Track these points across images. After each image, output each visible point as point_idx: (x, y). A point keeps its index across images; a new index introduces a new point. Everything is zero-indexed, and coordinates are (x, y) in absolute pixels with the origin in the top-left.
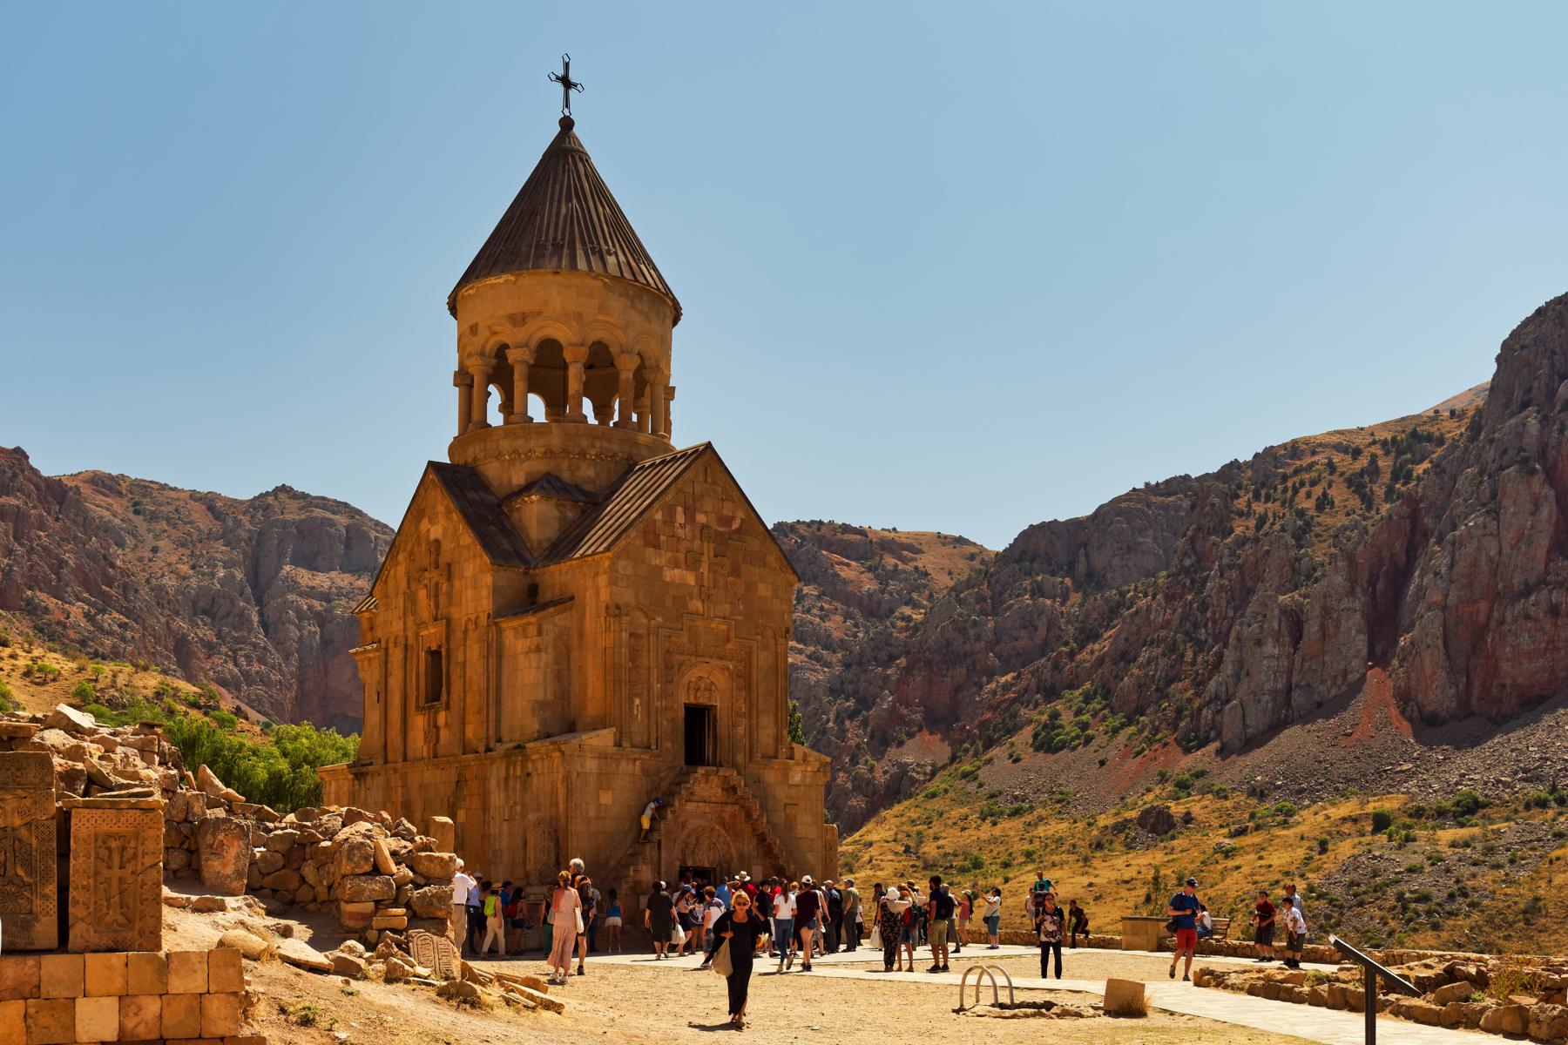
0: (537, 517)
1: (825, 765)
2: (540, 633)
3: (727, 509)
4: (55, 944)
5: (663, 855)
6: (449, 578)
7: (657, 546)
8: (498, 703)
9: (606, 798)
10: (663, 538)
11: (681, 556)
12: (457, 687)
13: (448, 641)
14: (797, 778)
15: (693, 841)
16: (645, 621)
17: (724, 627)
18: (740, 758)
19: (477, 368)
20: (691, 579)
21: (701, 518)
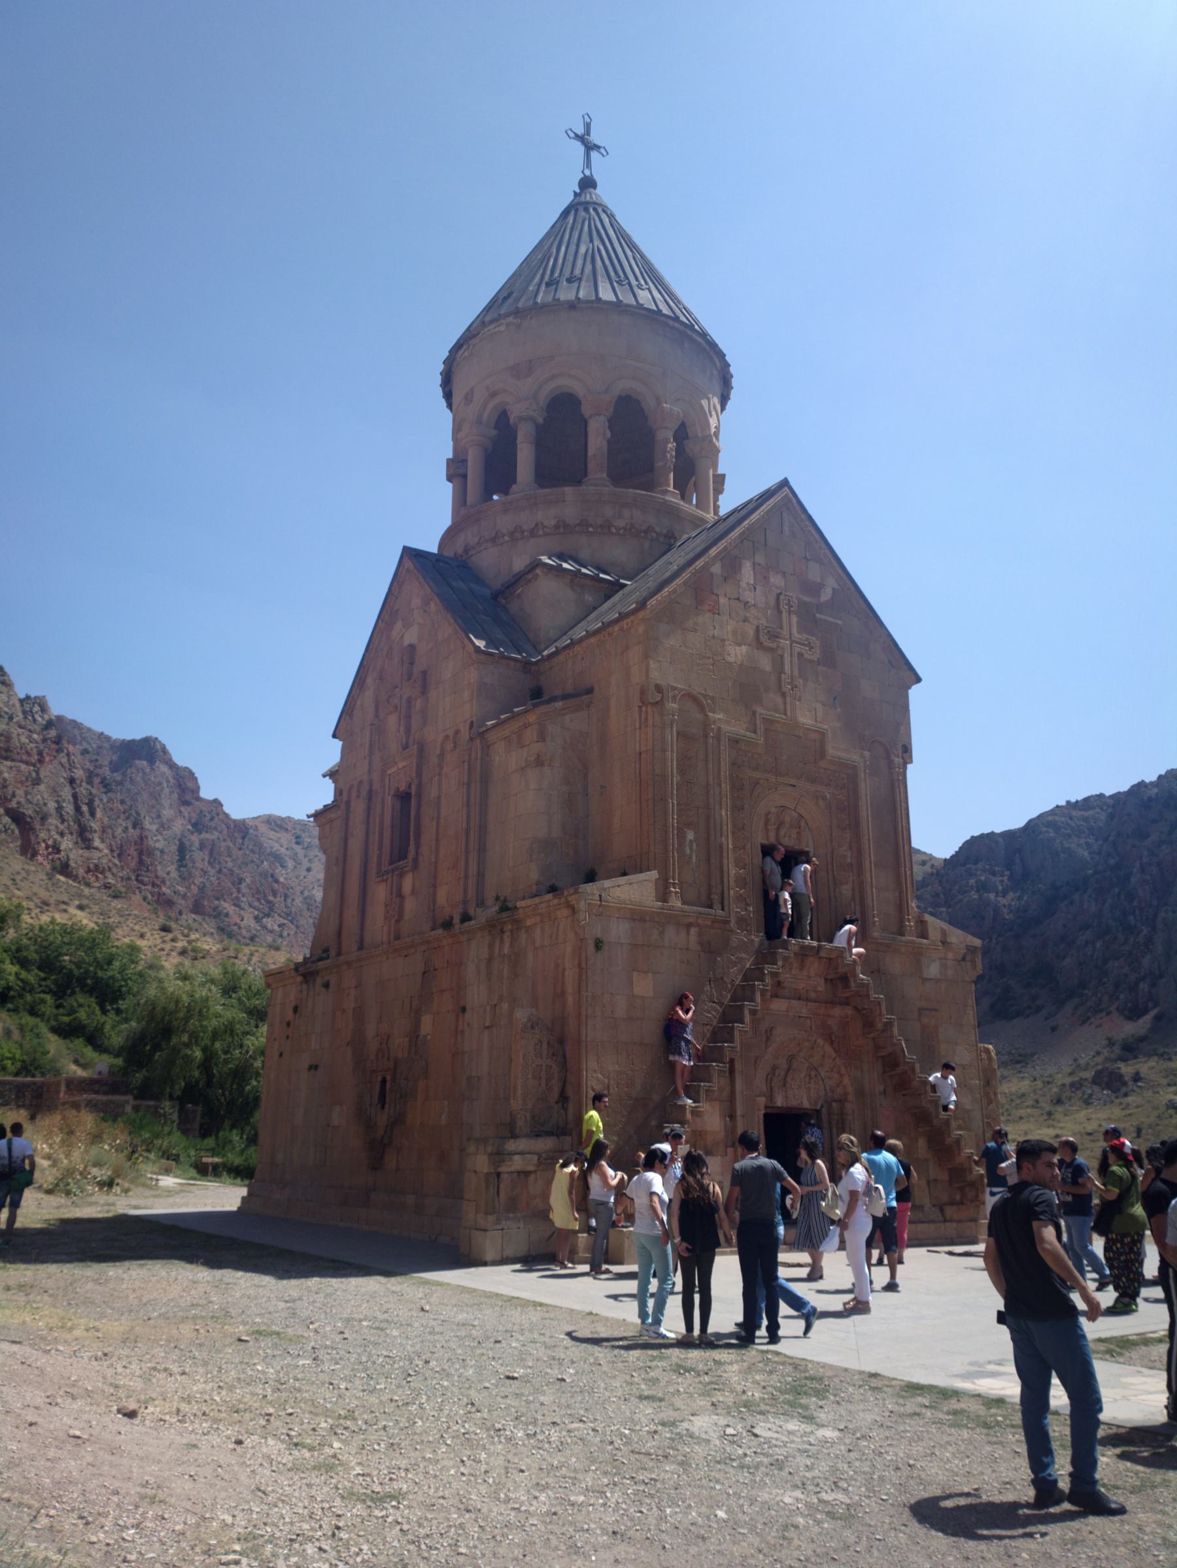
1: (971, 950)
2: (542, 737)
3: (814, 573)
5: (739, 1085)
6: (424, 691)
8: (482, 849)
10: (722, 600)
12: (428, 836)
13: (419, 773)
15: (782, 1062)
16: (699, 716)
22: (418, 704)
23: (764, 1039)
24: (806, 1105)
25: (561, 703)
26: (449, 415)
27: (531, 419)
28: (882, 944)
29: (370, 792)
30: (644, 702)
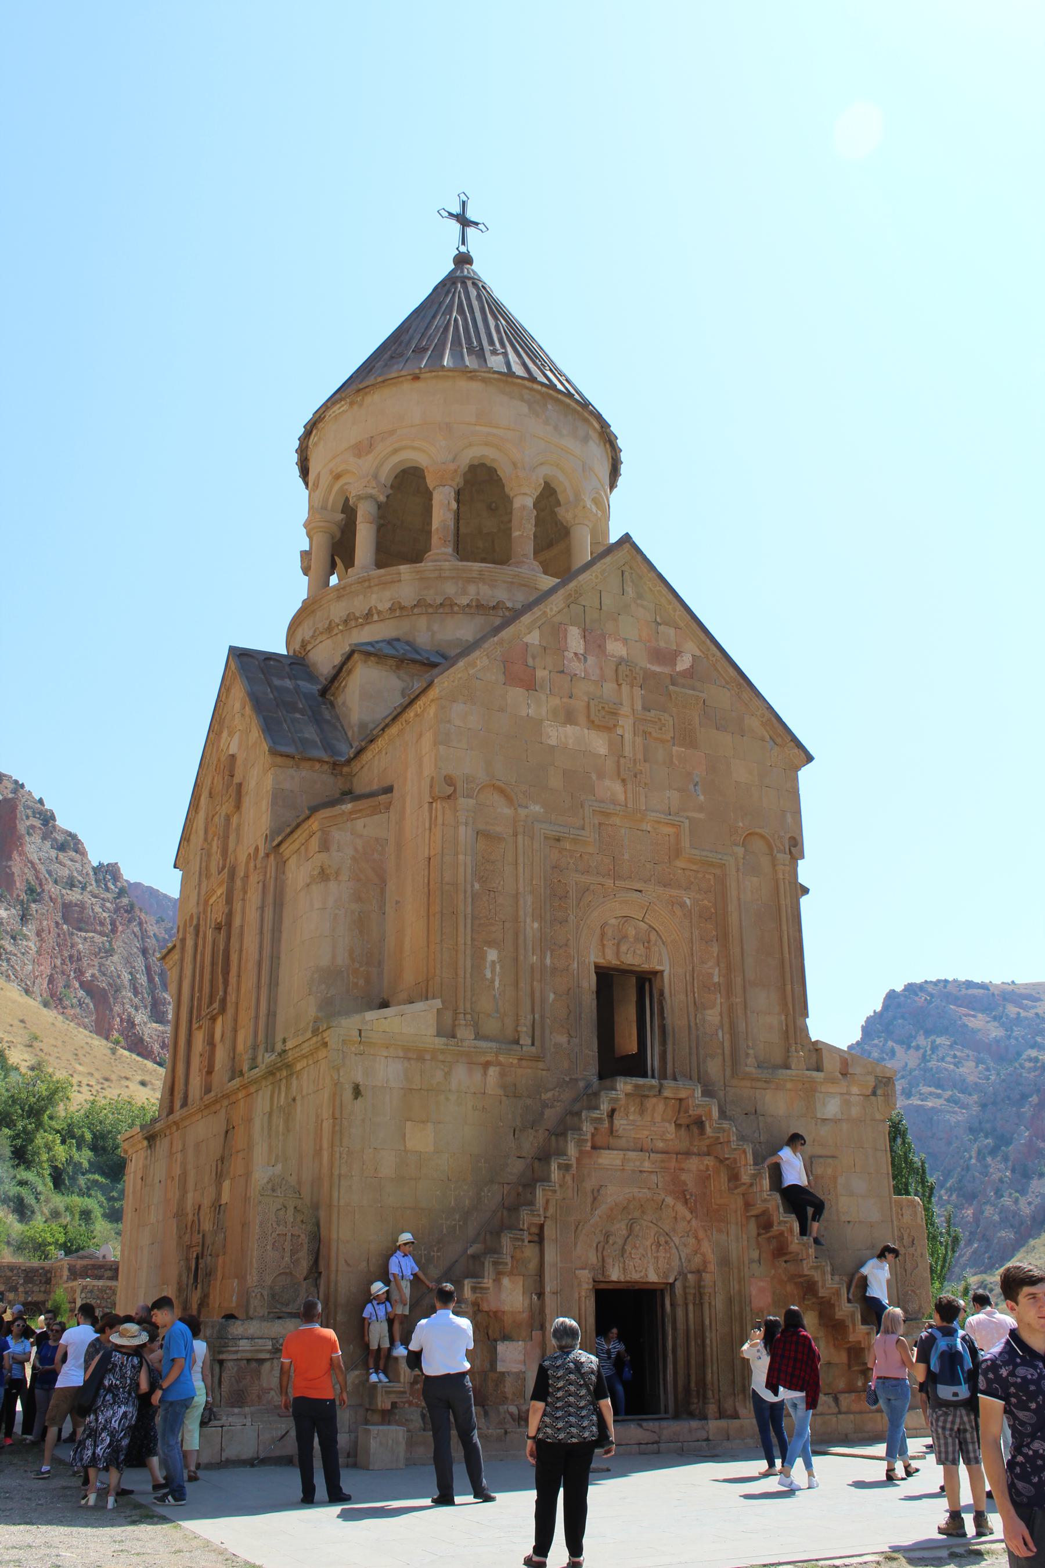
2: (325, 846)
3: (668, 636)
5: (551, 1254)
6: (238, 806)
7: (530, 685)
8: (274, 982)
9: (421, 1140)
10: (540, 674)
14: (831, 1108)
15: (620, 1228)
16: (508, 811)
18: (714, 1068)
20: (599, 744)
21: (615, 648)
22: (235, 820)
23: (589, 1200)
24: (653, 1277)
25: (349, 806)
28: (759, 1080)
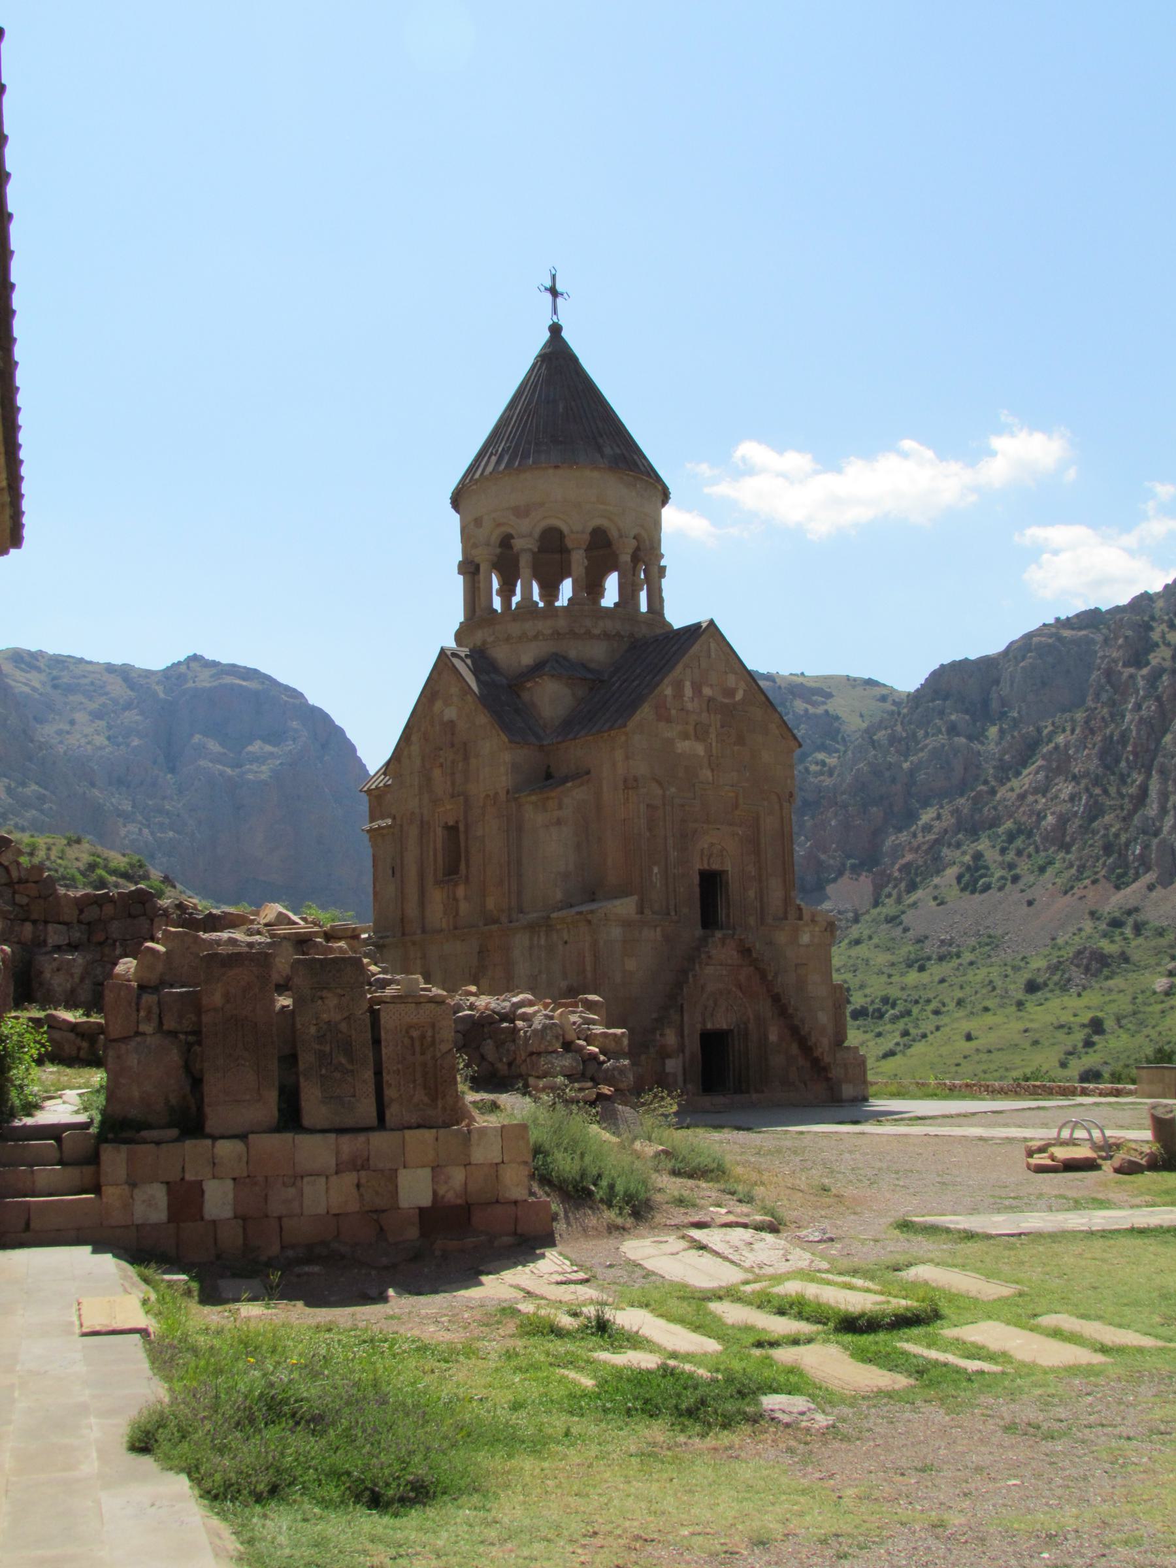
0: (551, 698)
3: (731, 680)
4: (372, 1119)
5: (686, 1018)
6: (466, 758)
7: (669, 720)
9: (631, 965)
10: (673, 712)
11: (691, 729)
14: (805, 938)
16: (660, 792)
17: (731, 794)
19: (483, 556)
20: (700, 749)
21: (707, 691)
24: (725, 1027)
26: (456, 517)
27: (530, 550)
29: (422, 822)
30: (626, 788)
